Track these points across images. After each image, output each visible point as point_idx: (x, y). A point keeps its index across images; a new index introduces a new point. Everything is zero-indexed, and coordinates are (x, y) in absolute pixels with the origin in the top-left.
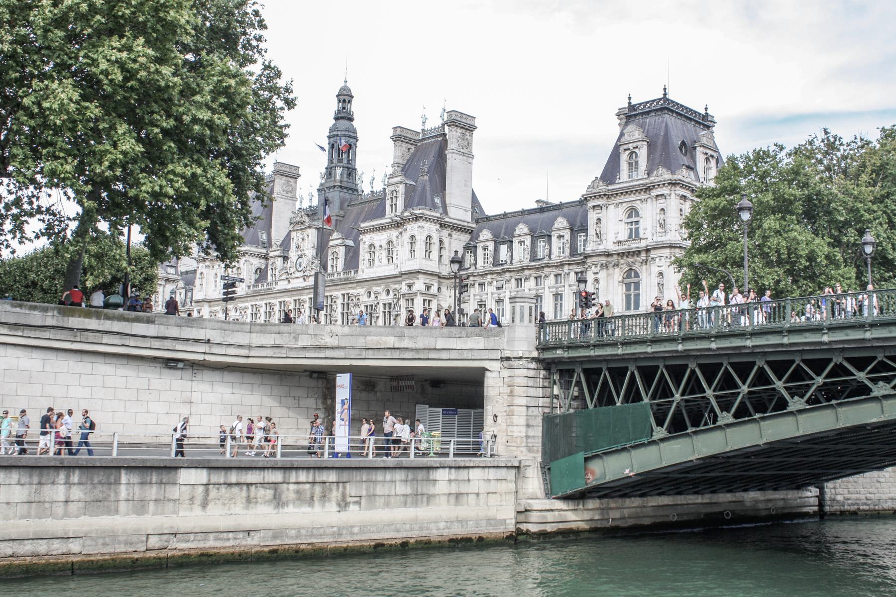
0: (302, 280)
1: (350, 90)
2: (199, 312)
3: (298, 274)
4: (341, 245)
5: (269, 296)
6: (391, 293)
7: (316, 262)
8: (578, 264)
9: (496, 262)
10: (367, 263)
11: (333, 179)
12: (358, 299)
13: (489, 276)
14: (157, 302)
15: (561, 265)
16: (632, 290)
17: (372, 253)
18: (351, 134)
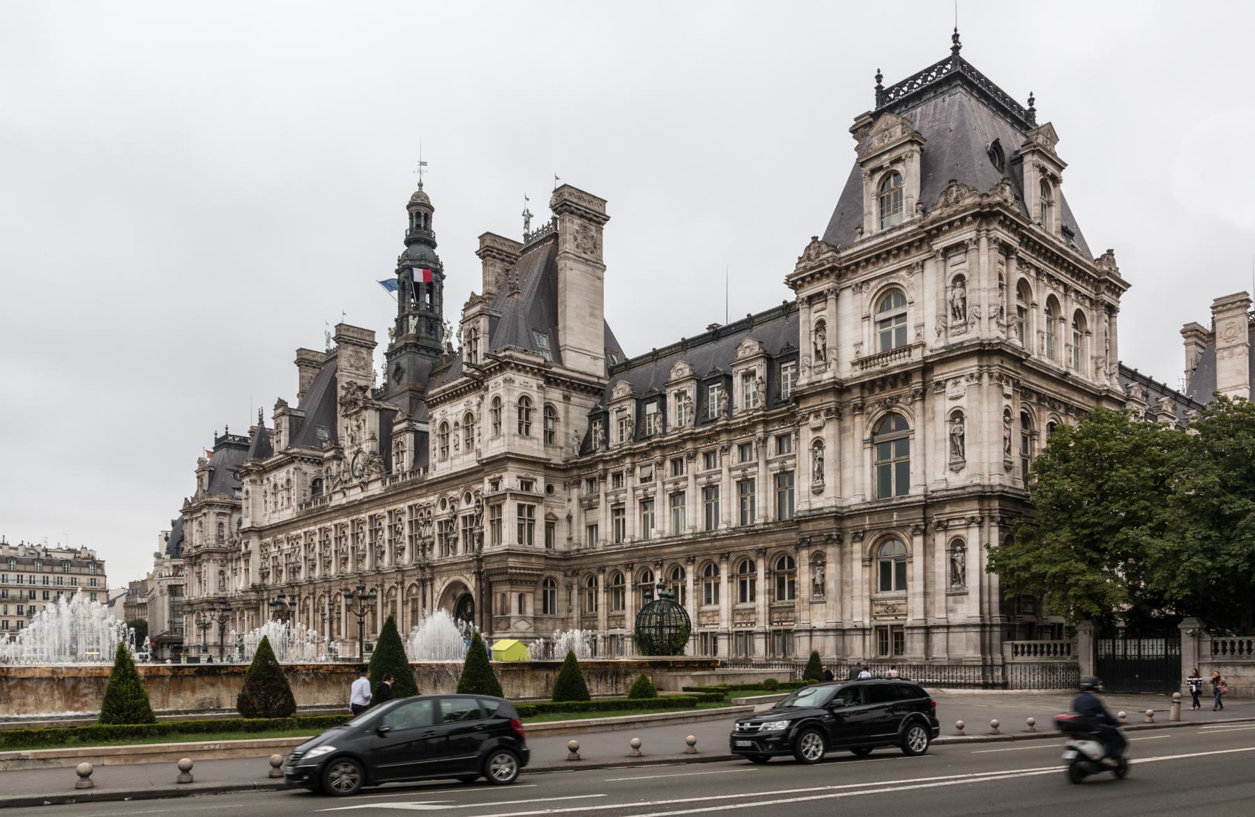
0: (359, 489)
2: (246, 546)
3: (355, 482)
4: (406, 430)
5: (323, 518)
6: (473, 497)
7: (376, 460)
8: (782, 420)
9: (639, 432)
10: (438, 452)
12: (429, 513)
13: (628, 460)
14: (222, 537)
15: (749, 427)
16: (893, 455)
17: (444, 437)
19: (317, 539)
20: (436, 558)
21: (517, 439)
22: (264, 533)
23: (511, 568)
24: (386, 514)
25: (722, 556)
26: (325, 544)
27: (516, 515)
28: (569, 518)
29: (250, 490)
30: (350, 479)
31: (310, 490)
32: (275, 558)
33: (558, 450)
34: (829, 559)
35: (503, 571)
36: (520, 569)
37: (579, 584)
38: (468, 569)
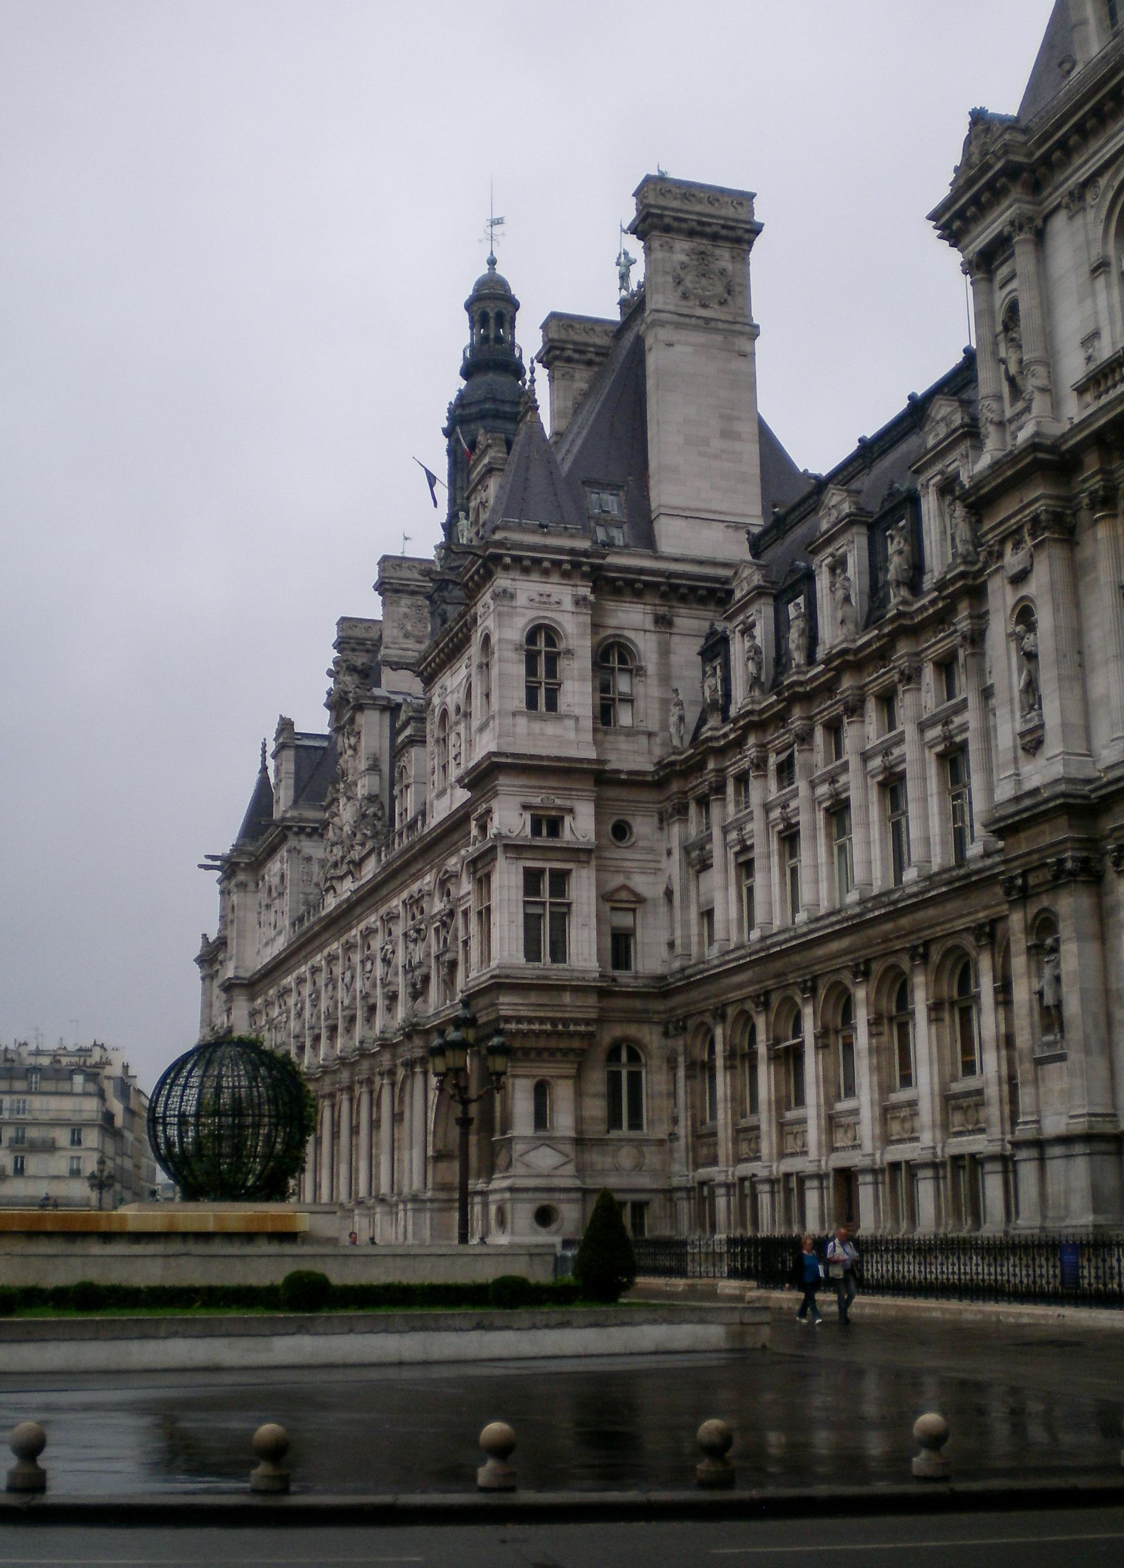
1: (502, 283)
18: (507, 408)
21: (522, 721)
23: (507, 1019)
25: (913, 952)
27: (518, 895)
28: (669, 894)
33: (643, 740)
34: (1065, 929)
36: (530, 1020)
37: (687, 1052)
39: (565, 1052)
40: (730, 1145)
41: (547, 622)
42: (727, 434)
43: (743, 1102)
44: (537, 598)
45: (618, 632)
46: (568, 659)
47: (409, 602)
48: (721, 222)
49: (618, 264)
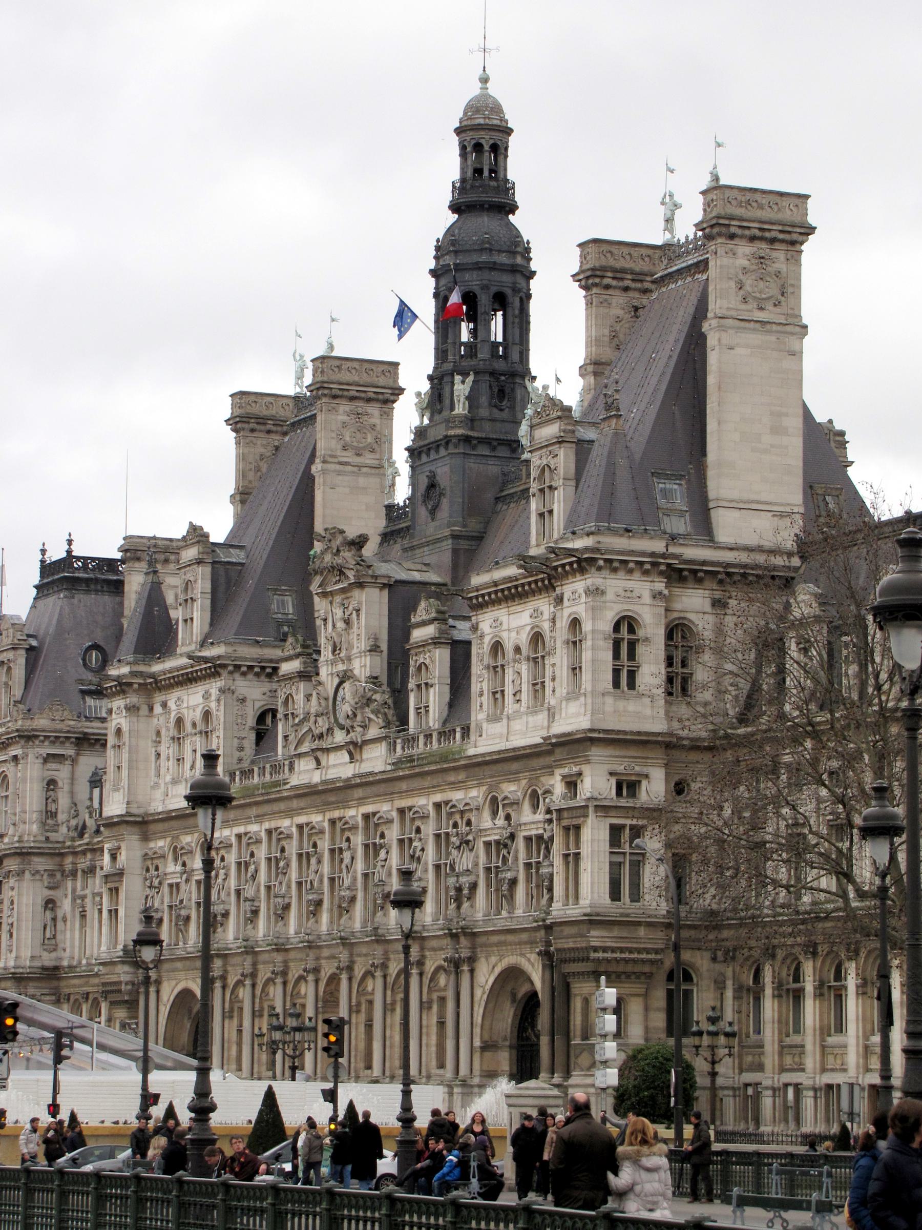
0: (346, 757)
1: (497, 109)
2: (114, 857)
3: (340, 737)
4: (436, 642)
5: (276, 807)
7: (377, 697)
11: (446, 413)
12: (469, 823)
14: (54, 815)
17: (497, 670)
18: (503, 259)
19: (262, 852)
20: (479, 916)
21: (609, 700)
22: (152, 827)
23: (596, 949)
24: (394, 814)
26: (277, 864)
27: (606, 847)
29: (125, 728)
30: (330, 730)
31: (253, 736)
32: (176, 886)
35: (581, 955)
36: (613, 950)
38: (532, 942)
39: (638, 975)
40: (776, 1057)
41: (630, 614)
42: (777, 430)
43: (787, 1024)
44: (623, 594)
45: (682, 615)
46: (646, 646)
47: (347, 408)
48: (780, 228)
49: (663, 203)
